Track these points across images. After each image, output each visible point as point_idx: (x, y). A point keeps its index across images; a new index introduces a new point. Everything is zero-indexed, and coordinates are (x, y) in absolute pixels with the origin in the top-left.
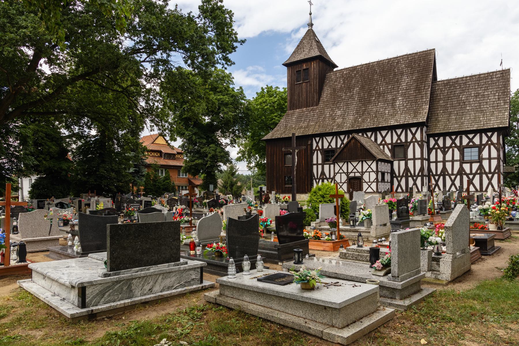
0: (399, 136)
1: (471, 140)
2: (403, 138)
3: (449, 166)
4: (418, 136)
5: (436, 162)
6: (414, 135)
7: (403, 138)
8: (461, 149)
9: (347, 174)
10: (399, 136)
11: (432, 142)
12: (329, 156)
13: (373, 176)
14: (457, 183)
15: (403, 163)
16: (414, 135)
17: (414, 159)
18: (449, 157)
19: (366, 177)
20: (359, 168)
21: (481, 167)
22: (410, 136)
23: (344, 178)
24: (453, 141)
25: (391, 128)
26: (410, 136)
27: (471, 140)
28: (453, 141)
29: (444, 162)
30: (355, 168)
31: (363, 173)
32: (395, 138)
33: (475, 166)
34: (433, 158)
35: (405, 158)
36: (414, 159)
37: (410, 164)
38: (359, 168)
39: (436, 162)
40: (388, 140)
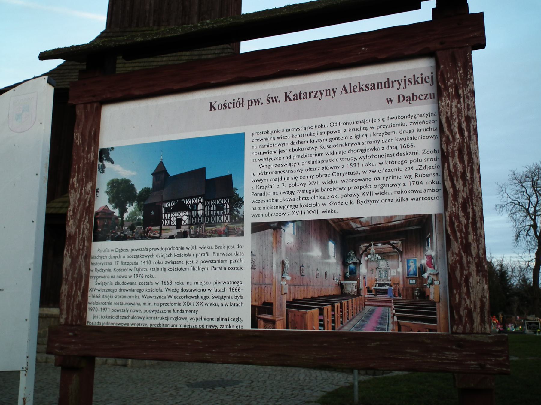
0: (194, 201)
1: (220, 202)
2: (196, 201)
3: (212, 212)
4: (202, 200)
5: (207, 211)
6: (200, 200)
7: (196, 201)
8: (216, 205)
9: (176, 217)
10: (194, 201)
11: (206, 203)
12: (168, 210)
13: (187, 217)
14: (215, 219)
15: (196, 212)
16: (200, 200)
17: (200, 210)
18: (212, 209)
19: (183, 218)
20: (181, 214)
21: (224, 212)
22: (199, 201)
23: (175, 219)
24: (214, 202)
25: (191, 198)
26: (199, 201)
27: (220, 202)
28: (214, 202)
29: (210, 211)
30: (179, 215)
31: (182, 216)
32: (193, 201)
33: (222, 212)
34: (206, 210)
35: (197, 210)
36: (200, 210)
37: (199, 212)
38: (181, 214)
39: (207, 211)
40: (190, 202)
